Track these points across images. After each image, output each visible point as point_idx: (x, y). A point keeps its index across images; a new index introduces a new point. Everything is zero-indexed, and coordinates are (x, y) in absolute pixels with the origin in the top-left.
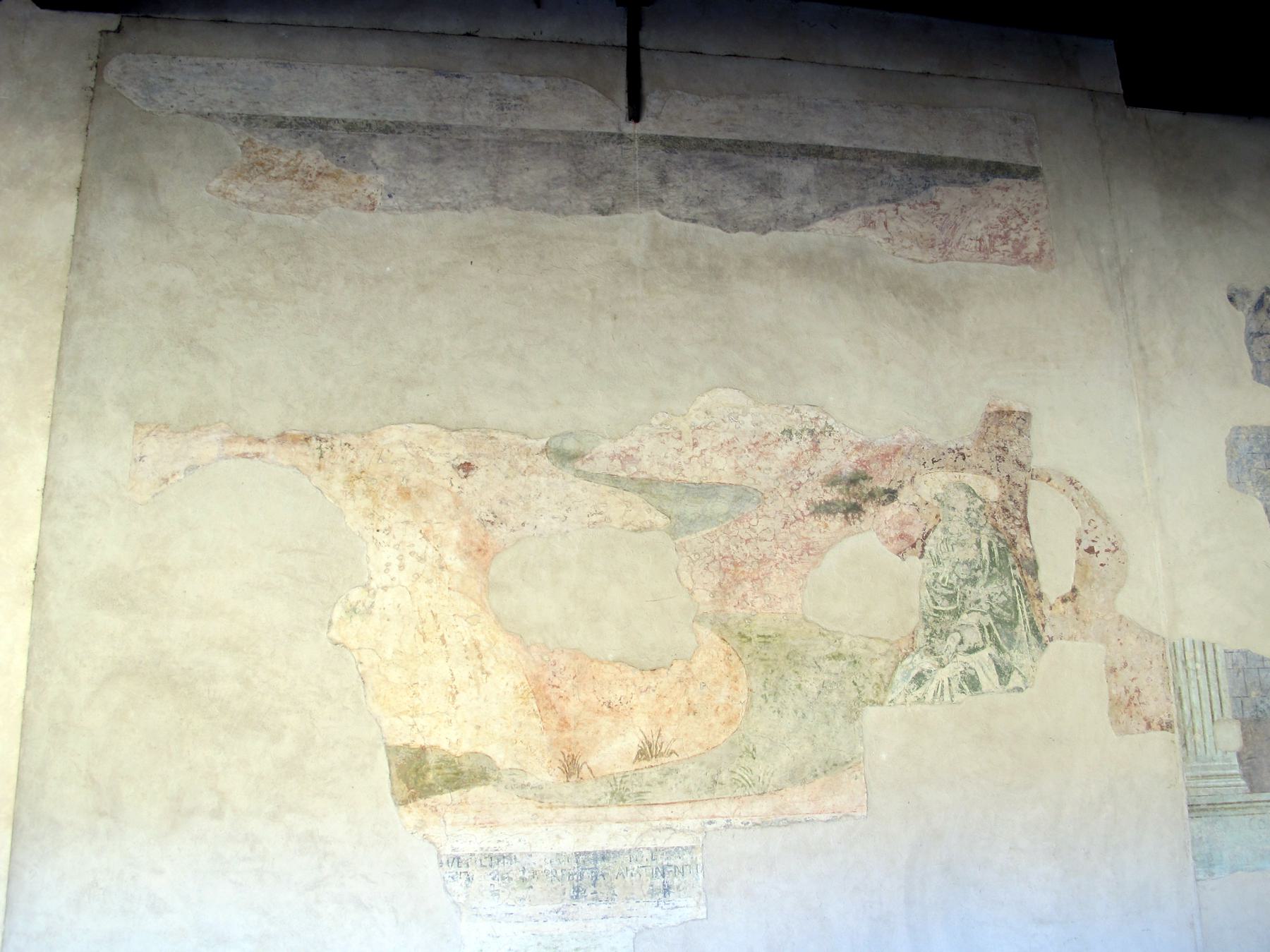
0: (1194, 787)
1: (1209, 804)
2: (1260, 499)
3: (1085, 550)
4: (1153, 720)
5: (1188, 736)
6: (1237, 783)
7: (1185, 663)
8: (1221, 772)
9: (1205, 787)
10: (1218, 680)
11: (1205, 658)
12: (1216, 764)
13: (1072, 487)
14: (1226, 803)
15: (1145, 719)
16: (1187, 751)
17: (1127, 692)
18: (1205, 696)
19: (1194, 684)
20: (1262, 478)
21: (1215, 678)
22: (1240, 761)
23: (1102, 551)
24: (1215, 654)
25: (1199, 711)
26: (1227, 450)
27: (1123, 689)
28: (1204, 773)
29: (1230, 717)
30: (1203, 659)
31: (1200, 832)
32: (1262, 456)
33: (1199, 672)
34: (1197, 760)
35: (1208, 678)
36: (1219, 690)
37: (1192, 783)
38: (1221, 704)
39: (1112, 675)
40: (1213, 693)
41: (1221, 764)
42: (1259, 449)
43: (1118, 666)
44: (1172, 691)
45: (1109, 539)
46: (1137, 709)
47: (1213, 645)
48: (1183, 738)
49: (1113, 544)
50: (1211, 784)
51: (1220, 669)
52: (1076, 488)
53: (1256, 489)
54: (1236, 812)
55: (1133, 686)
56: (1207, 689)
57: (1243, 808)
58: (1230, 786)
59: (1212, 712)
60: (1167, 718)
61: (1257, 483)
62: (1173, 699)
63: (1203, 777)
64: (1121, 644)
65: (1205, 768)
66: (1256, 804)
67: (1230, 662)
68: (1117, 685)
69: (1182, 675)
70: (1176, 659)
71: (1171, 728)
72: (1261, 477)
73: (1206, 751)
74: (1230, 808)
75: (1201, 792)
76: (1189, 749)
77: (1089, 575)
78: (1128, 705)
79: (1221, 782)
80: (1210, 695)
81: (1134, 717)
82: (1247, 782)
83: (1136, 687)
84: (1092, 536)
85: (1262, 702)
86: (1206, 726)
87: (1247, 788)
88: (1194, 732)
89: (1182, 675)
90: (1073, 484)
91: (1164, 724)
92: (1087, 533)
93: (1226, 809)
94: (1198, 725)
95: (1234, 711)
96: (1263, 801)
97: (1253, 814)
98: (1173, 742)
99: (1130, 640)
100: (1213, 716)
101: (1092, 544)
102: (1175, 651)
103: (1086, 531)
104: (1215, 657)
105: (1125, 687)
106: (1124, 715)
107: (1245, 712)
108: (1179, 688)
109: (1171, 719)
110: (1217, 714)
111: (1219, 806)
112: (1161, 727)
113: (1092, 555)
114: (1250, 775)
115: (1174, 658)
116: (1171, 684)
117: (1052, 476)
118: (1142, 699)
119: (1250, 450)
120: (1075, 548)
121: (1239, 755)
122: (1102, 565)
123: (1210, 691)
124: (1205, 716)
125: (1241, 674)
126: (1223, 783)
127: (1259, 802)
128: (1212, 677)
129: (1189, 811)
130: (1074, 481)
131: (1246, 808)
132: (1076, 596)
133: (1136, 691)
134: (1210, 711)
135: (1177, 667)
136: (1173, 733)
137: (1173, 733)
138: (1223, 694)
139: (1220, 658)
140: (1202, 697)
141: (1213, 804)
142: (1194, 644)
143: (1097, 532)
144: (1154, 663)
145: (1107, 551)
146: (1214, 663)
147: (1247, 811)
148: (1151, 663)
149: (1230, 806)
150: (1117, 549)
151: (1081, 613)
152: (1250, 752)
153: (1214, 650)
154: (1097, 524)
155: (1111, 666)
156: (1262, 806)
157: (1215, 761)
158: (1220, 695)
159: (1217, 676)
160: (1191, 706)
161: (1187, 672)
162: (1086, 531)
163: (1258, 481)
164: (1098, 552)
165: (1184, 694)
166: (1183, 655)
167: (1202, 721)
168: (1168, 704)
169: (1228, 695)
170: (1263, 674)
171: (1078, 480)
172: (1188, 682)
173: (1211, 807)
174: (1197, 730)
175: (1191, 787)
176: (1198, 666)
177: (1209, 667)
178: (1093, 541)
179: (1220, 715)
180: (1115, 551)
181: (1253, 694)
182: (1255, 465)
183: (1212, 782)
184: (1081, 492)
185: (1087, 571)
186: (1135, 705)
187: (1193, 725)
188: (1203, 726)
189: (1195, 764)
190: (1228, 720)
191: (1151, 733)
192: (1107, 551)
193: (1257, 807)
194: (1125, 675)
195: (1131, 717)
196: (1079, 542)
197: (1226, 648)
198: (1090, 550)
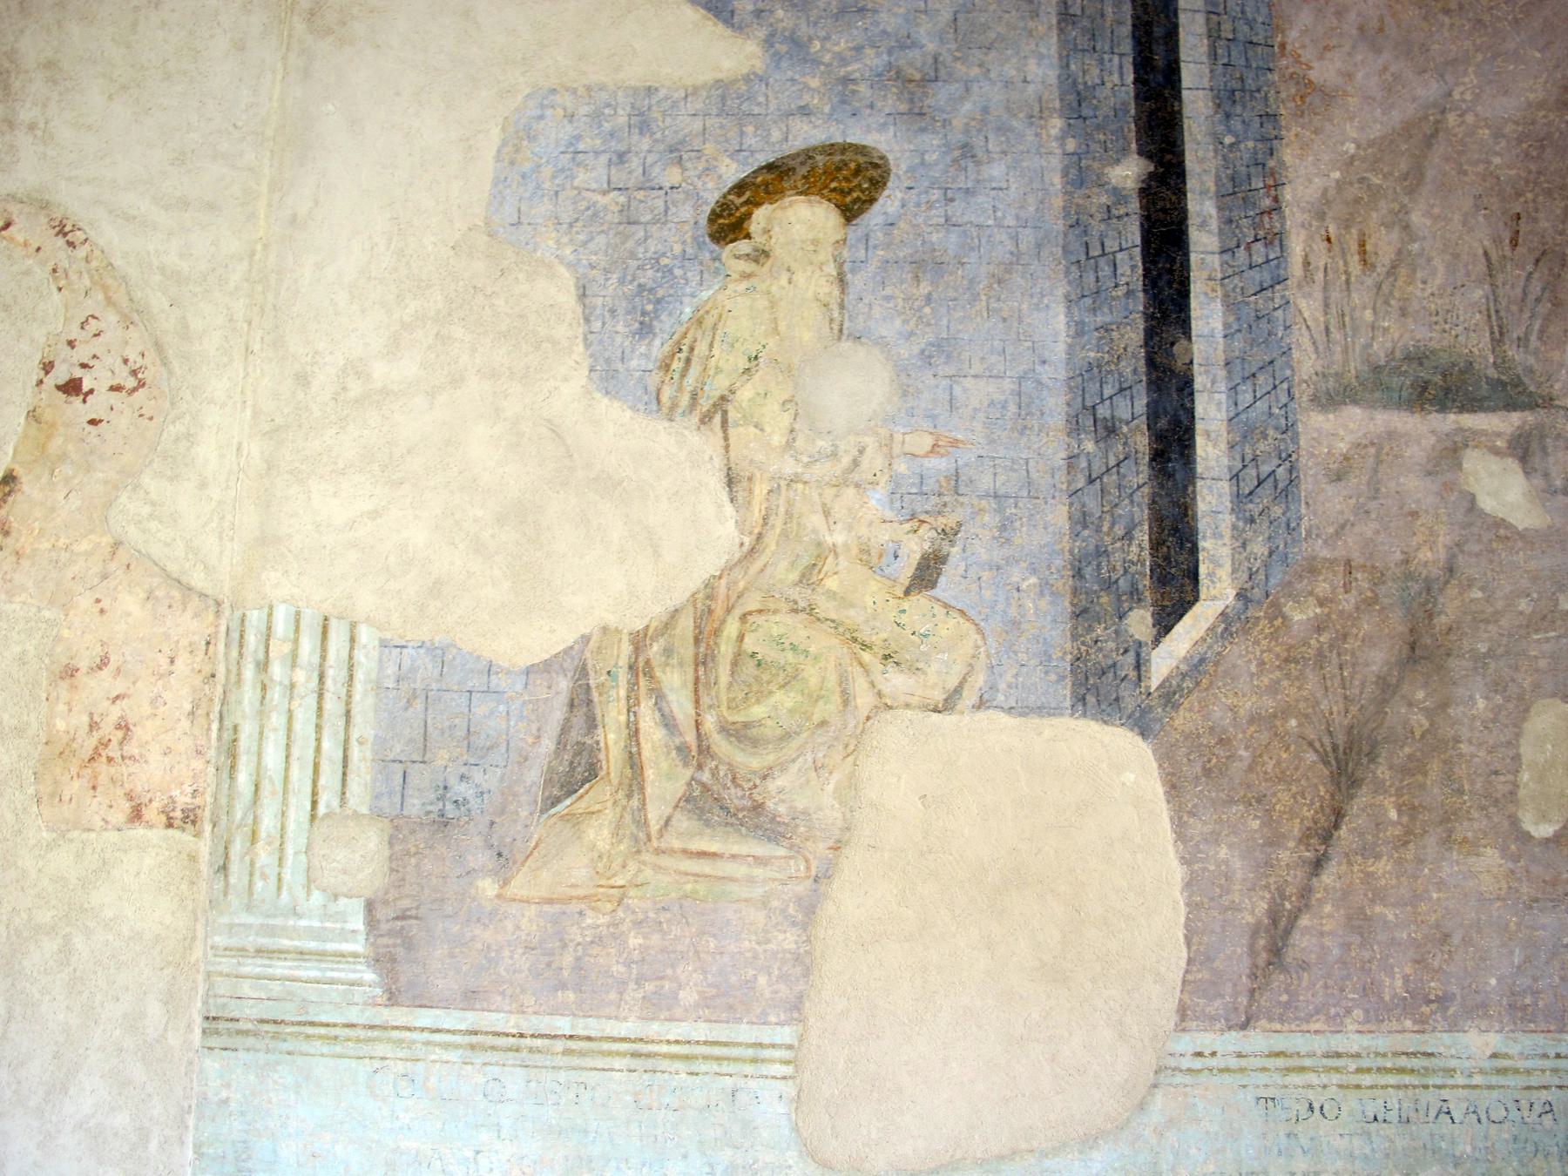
0: (228, 975)
1: (262, 1021)
2: (569, 265)
3: (59, 388)
4: (151, 801)
5: (237, 848)
6: (352, 976)
7: (263, 666)
8: (312, 945)
9: (259, 978)
10: (348, 713)
11: (323, 658)
12: (303, 923)
13: (61, 241)
14: (312, 1024)
15: (129, 796)
16: (227, 885)
17: (93, 726)
18: (303, 750)
19: (277, 720)
20: (589, 213)
21: (341, 709)
22: (372, 922)
23: (102, 387)
24: (352, 649)
25: (279, 788)
26: (504, 143)
27: (85, 719)
28: (264, 941)
29: (364, 810)
30: (316, 659)
31: (228, 1085)
32: (604, 159)
33: (300, 690)
34: (249, 908)
35: (320, 709)
36: (346, 741)
37: (226, 964)
38: (344, 774)
39: (64, 685)
40: (326, 745)
41: (316, 924)
42: (598, 142)
43: (83, 665)
44: (214, 735)
45: (126, 361)
46: (112, 770)
47: (353, 626)
48: (221, 849)
49: (134, 373)
50: (279, 972)
51: (359, 688)
52: (71, 244)
53: (565, 240)
54: (338, 1049)
55: (115, 712)
56: (313, 736)
57: (358, 1040)
58: (332, 982)
59: (314, 793)
60: (188, 799)
61: (571, 225)
62: (212, 753)
63: (260, 952)
64: (102, 611)
65: (271, 931)
66: (396, 1034)
67: (391, 670)
68: (70, 710)
69: (249, 694)
70: (241, 655)
71: (194, 822)
72: (588, 209)
73: (279, 889)
74: (321, 1037)
75: (246, 989)
76: (232, 880)
77: (56, 444)
78: (92, 759)
79: (306, 969)
80: (318, 749)
81: (100, 789)
82: (381, 976)
83: (122, 717)
84: (82, 353)
85: (462, 777)
86: (291, 827)
87: (379, 991)
88: (254, 837)
89: (249, 694)
90: (65, 235)
91: (178, 814)
92: (73, 347)
93: (308, 1037)
94: (268, 823)
95: (377, 797)
96: (423, 1030)
97: (383, 1059)
98: (193, 858)
99: (130, 603)
100: (314, 803)
101: (78, 373)
102: (242, 637)
103: (71, 344)
104: (351, 657)
105: (91, 715)
106: (76, 784)
107: (409, 801)
108: (235, 728)
109: (198, 801)
110: (327, 800)
111: (289, 1029)
112: (169, 818)
113: (72, 399)
114: (393, 960)
115: (234, 654)
116: (215, 716)
117: (15, 217)
118: (132, 749)
119: (572, 144)
120: (35, 379)
121: (370, 907)
122: (93, 422)
123: (318, 740)
124: (293, 800)
125: (419, 705)
126: (313, 974)
127: (409, 1029)
128: (332, 705)
129: (204, 1032)
130: (67, 229)
131: (368, 1040)
132: (9, 493)
133: (118, 727)
134: (309, 790)
135: (239, 674)
136: (197, 835)
137: (197, 835)
138: (355, 753)
139: (366, 662)
140: (295, 752)
141: (275, 1022)
142: (297, 622)
143: (97, 346)
144: (179, 662)
145: (116, 388)
146: (345, 673)
147: (366, 1049)
148: (172, 662)
149: (323, 1031)
150: (141, 384)
151: (14, 534)
152: (405, 903)
153: (352, 640)
154: (102, 325)
155: (65, 661)
156: (414, 1042)
157: (300, 916)
158: (345, 750)
159: (348, 703)
160: (258, 775)
161: (264, 688)
162: (71, 344)
163: (577, 220)
164: (91, 391)
165: (245, 742)
166: (262, 649)
167: (283, 813)
168: (198, 764)
169: (369, 755)
170: (480, 710)
171: (81, 224)
172: (262, 712)
173: (266, 1027)
174: (263, 834)
175: (221, 974)
176: (300, 676)
177: (329, 683)
178: (84, 366)
179: (336, 803)
180: (135, 390)
181: (441, 757)
182: (576, 182)
183: (281, 968)
184: (81, 252)
185: (49, 437)
186: (110, 760)
187: (256, 820)
188: (283, 828)
189: (245, 918)
190: (356, 815)
191: (139, 832)
192: (116, 388)
193: (400, 1042)
194: (98, 687)
195: (94, 788)
196: (48, 367)
197: (388, 635)
198: (72, 387)
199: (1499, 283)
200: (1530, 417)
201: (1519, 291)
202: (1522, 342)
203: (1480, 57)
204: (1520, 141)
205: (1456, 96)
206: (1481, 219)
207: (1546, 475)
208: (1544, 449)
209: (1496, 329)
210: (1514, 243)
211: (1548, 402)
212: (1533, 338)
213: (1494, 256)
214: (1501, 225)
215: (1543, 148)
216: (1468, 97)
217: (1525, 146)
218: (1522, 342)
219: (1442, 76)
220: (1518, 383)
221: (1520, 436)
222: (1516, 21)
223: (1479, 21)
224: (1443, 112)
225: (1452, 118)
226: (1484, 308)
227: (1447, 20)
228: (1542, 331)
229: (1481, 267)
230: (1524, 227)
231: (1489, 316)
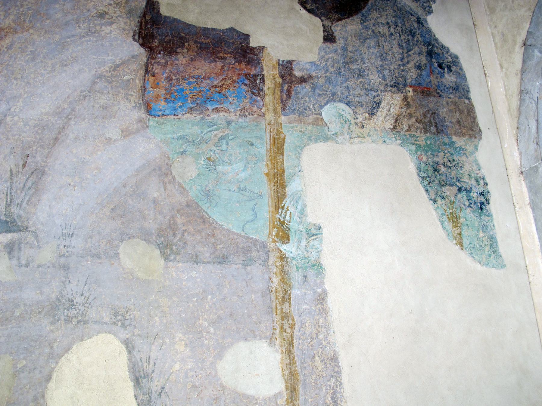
199: (14, 182)
200: (16, 235)
201: (22, 185)
202: (20, 205)
203: (26, 95)
204: (35, 127)
205: (12, 110)
206: (12, 157)
207: (19, 259)
208: (20, 249)
209: (9, 200)
210: (24, 166)
211: (26, 229)
212: (24, 204)
213: (14, 171)
214: (20, 159)
215: (44, 129)
216: (17, 110)
217: (36, 129)
218: (20, 205)
219: (8, 102)
220: (14, 222)
221: (10, 243)
222: (44, 83)
223: (28, 83)
224: (5, 116)
225: (8, 119)
226: (5, 192)
227: (15, 82)
228: (28, 201)
229: (8, 175)
230: (29, 160)
231: (7, 195)
